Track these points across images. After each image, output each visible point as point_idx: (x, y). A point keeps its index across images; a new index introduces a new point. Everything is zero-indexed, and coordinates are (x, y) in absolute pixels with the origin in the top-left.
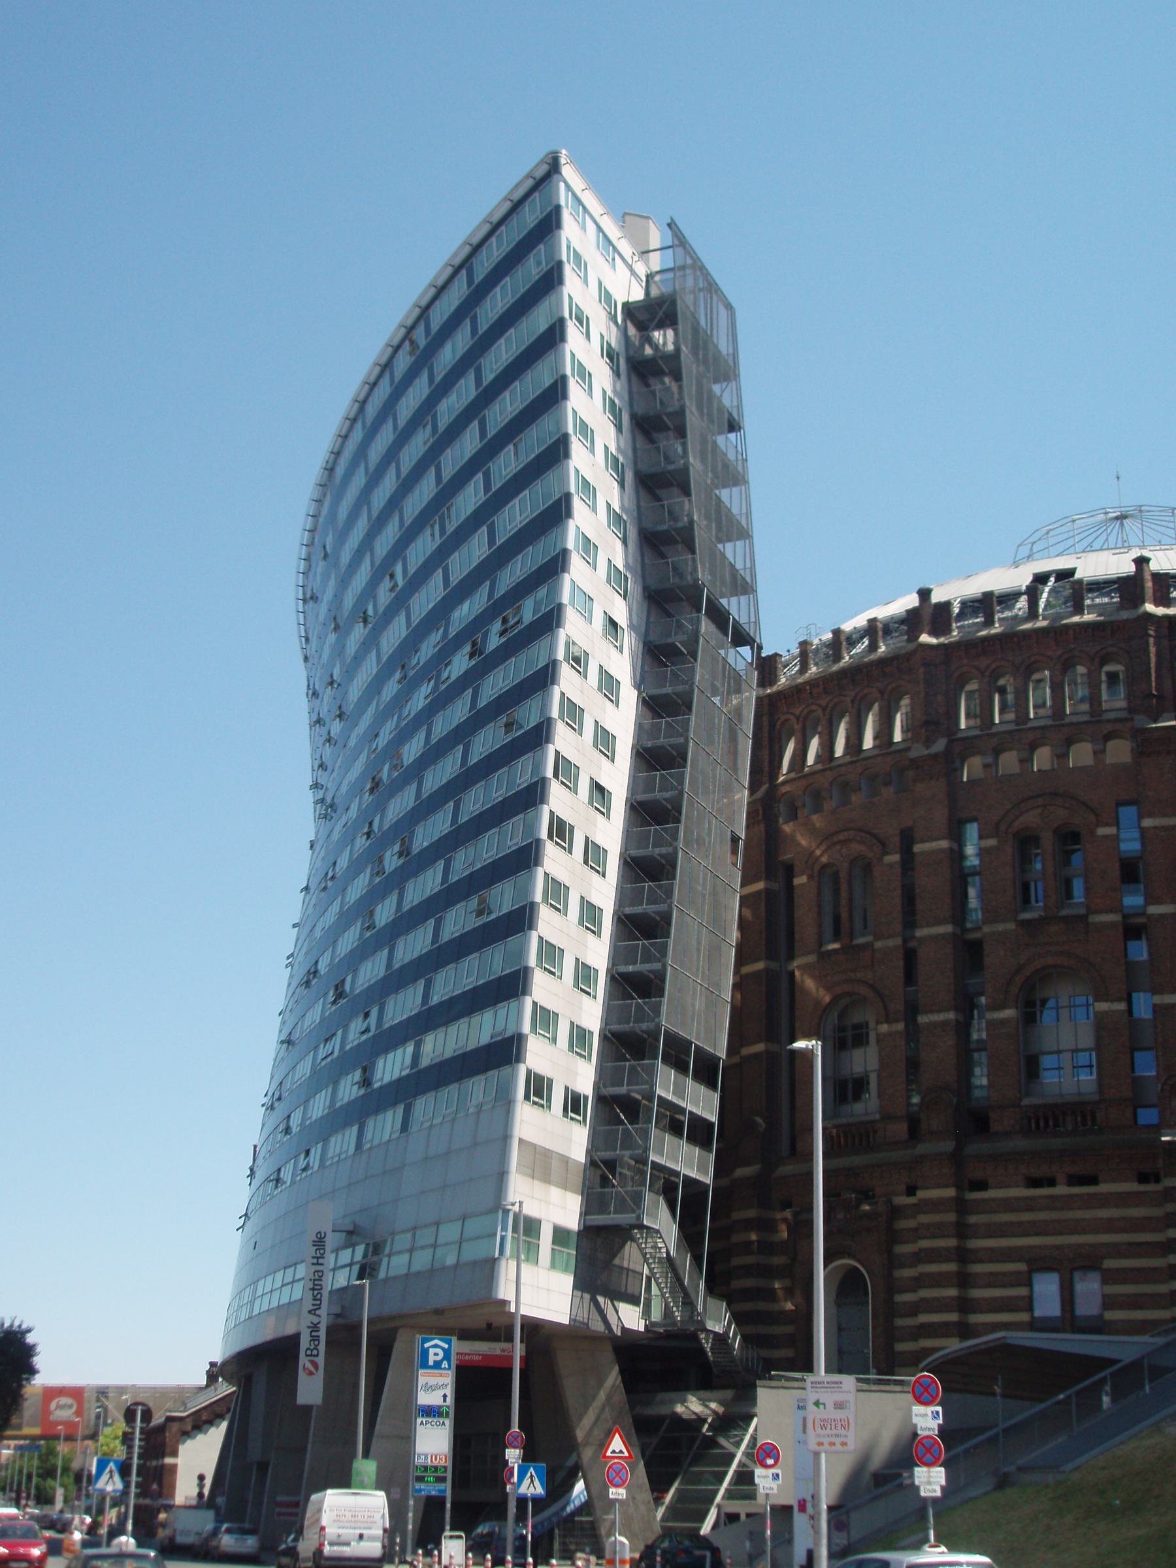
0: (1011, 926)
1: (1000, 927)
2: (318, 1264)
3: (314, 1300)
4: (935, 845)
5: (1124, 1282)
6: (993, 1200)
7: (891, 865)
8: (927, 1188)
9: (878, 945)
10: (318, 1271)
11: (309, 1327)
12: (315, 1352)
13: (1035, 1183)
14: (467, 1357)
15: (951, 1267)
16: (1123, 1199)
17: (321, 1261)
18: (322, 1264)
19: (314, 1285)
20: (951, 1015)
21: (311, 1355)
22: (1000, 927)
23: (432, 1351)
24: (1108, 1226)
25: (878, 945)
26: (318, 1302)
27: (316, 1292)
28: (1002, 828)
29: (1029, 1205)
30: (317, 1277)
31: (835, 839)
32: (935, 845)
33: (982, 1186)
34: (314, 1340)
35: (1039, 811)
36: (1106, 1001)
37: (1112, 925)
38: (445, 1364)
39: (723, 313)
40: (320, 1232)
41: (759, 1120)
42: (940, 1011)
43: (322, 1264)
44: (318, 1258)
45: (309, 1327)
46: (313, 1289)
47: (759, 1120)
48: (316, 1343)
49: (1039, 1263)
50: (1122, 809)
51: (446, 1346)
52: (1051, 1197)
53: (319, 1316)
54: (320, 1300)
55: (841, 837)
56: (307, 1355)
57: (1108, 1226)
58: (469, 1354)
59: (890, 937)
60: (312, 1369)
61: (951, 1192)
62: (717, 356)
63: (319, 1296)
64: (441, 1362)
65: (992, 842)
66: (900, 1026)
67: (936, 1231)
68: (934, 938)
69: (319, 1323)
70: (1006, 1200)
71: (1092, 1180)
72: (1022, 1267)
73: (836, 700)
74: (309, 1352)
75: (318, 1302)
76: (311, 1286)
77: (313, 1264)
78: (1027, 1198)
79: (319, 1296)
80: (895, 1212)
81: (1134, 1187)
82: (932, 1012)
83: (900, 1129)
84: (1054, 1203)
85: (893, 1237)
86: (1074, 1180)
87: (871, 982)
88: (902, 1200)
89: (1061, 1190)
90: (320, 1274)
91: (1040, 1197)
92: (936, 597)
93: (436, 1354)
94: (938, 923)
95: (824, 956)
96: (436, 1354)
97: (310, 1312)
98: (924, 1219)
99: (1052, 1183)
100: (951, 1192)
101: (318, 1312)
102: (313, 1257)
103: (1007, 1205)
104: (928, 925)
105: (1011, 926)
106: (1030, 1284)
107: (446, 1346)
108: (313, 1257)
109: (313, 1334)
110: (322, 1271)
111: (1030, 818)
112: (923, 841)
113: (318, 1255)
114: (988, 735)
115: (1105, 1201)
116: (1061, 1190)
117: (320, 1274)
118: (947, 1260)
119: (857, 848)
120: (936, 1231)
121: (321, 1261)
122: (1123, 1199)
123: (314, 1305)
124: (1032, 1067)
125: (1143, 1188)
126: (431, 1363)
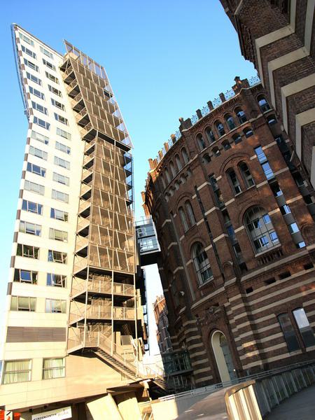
0: (233, 200)
15: (248, 323)
20: (223, 236)
25: (198, 224)
29: (268, 291)
33: (250, 290)
37: (265, 185)
50: (256, 150)
52: (276, 286)
61: (240, 296)
66: (211, 246)
67: (239, 311)
70: (260, 292)
71: (288, 275)
78: (266, 290)
80: (225, 309)
83: (221, 279)
84: (278, 288)
85: (228, 318)
86: (282, 277)
88: (226, 305)
89: (278, 282)
92: (184, 120)
95: (185, 234)
98: (233, 309)
99: (273, 281)
100: (240, 296)
111: (229, 165)
115: (295, 280)
116: (278, 282)
118: (246, 321)
119: (186, 198)
120: (239, 311)
124: (257, 245)
125: (308, 271)
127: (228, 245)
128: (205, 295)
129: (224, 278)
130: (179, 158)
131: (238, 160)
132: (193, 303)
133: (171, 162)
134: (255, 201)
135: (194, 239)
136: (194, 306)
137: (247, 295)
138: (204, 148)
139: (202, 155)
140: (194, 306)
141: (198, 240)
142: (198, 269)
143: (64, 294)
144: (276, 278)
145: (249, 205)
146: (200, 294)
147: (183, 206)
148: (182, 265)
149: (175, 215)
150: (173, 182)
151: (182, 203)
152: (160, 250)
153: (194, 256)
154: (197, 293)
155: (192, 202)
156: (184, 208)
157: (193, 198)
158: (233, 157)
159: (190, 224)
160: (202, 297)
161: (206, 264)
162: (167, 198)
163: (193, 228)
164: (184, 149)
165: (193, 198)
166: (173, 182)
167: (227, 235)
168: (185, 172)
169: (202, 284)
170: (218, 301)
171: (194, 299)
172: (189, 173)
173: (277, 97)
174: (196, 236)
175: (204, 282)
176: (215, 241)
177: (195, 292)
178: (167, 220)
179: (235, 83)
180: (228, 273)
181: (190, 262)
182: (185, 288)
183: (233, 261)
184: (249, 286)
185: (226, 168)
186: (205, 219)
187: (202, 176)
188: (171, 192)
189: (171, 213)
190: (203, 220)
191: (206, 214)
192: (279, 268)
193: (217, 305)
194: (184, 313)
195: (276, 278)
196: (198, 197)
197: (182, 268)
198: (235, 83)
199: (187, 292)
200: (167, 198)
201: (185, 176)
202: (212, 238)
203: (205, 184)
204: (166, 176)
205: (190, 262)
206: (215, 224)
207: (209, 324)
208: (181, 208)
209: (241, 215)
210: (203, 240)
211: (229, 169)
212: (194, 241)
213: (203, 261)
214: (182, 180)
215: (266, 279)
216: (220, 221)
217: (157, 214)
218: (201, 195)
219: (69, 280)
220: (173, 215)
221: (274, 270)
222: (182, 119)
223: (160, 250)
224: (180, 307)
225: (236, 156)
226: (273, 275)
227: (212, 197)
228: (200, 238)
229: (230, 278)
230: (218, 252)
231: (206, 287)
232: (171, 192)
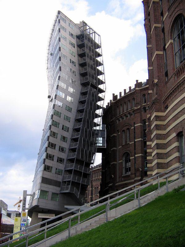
20: (141, 155)
25: (130, 143)
39: (97, 35)
41: (113, 176)
47: (113, 176)
62: (95, 44)
66: (134, 157)
83: (134, 175)
92: (139, 82)
95: (122, 146)
119: (128, 127)
127: (142, 160)
128: (124, 181)
129: (135, 176)
130: (130, 102)
132: (117, 183)
133: (125, 102)
136: (117, 184)
138: (145, 103)
139: (142, 107)
140: (117, 184)
141: (128, 151)
142: (124, 166)
143: (62, 167)
146: (122, 179)
147: (125, 130)
148: (116, 162)
149: (119, 133)
151: (125, 128)
152: (106, 147)
153: (124, 159)
154: (120, 178)
156: (125, 132)
157: (132, 128)
159: (126, 142)
160: (122, 181)
161: (129, 165)
162: (117, 121)
163: (127, 144)
164: (134, 99)
165: (132, 128)
167: (143, 155)
168: (131, 112)
169: (124, 175)
171: (118, 181)
172: (133, 114)
173: (180, 103)
174: (128, 149)
175: (125, 173)
176: (136, 156)
177: (119, 178)
178: (115, 135)
180: (138, 174)
181: (120, 161)
182: (115, 174)
183: (142, 169)
186: (135, 142)
188: (121, 119)
189: (118, 130)
190: (133, 142)
191: (136, 140)
194: (111, 187)
196: (134, 129)
197: (116, 163)
199: (115, 176)
200: (117, 121)
201: (131, 115)
202: (135, 154)
203: (140, 124)
204: (120, 109)
205: (120, 161)
206: (139, 148)
208: (124, 131)
210: (131, 153)
213: (128, 162)
214: (129, 115)
216: (141, 146)
217: (109, 127)
218: (136, 129)
219: (65, 161)
220: (118, 133)
223: (106, 147)
224: (109, 183)
227: (141, 133)
229: (138, 177)
230: (136, 162)
231: (124, 177)
232: (121, 119)
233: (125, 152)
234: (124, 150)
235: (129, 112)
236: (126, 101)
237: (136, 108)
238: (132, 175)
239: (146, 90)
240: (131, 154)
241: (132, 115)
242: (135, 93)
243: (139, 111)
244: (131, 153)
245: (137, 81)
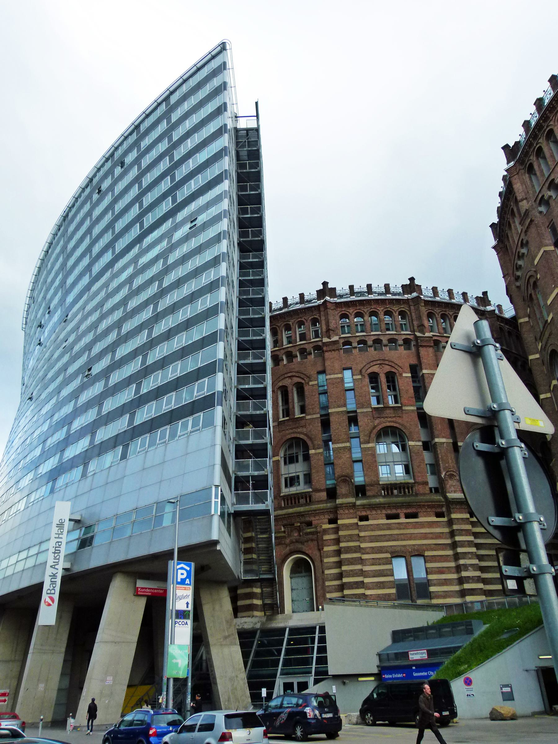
1: (365, 410)
2: (58, 538)
3: (54, 559)
4: (336, 376)
5: (435, 561)
6: (371, 525)
7: (313, 385)
8: (343, 519)
9: (308, 417)
10: (58, 542)
11: (50, 576)
12: (53, 591)
13: (389, 517)
14: (156, 591)
16: (431, 524)
17: (60, 536)
18: (62, 538)
19: (56, 550)
21: (50, 593)
22: (365, 410)
23: (180, 571)
24: (425, 536)
25: (308, 417)
26: (57, 561)
27: (56, 555)
28: (364, 371)
29: (389, 527)
30: (57, 546)
31: (286, 376)
32: (336, 376)
34: (53, 584)
35: (378, 366)
36: (413, 441)
38: (187, 581)
40: (61, 519)
42: (342, 442)
43: (62, 538)
44: (59, 534)
45: (50, 576)
46: (55, 553)
48: (54, 585)
49: (396, 554)
51: (188, 569)
53: (57, 569)
54: (59, 559)
55: (289, 375)
56: (47, 594)
57: (425, 536)
58: (157, 589)
59: (314, 414)
60: (51, 603)
63: (58, 557)
64: (185, 579)
65: (359, 377)
68: (338, 413)
69: (57, 573)
70: (378, 525)
71: (415, 516)
72: (389, 555)
73: (285, 323)
74: (49, 592)
75: (57, 561)
76: (54, 551)
77: (55, 538)
78: (387, 524)
79: (58, 557)
81: (435, 519)
82: (339, 443)
83: (324, 495)
84: (400, 526)
86: (407, 516)
87: (305, 433)
90: (60, 544)
91: (393, 523)
92: (330, 286)
93: (182, 574)
94: (339, 407)
96: (182, 574)
97: (51, 567)
99: (397, 517)
101: (56, 567)
102: (56, 534)
103: (379, 527)
104: (334, 408)
105: (370, 410)
106: (391, 563)
107: (188, 569)
108: (56, 534)
109: (52, 580)
110: (61, 542)
111: (375, 369)
112: (330, 374)
113: (60, 532)
114: (355, 336)
117: (60, 544)
121: (60, 536)
122: (431, 524)
123: (54, 562)
126: (179, 580)
131: (387, 369)
134: (399, 423)
135: (293, 433)
137: (361, 523)
139: (342, 341)
141: (302, 436)
144: (402, 515)
145: (388, 424)
150: (283, 351)
153: (282, 454)
155: (306, 388)
157: (311, 383)
158: (383, 362)
166: (283, 351)
168: (309, 348)
170: (312, 519)
179: (408, 282)
184: (364, 513)
185: (370, 371)
187: (337, 365)
191: (330, 411)
192: (408, 505)
193: (309, 524)
195: (402, 515)
198: (408, 282)
207: (292, 542)
209: (375, 431)
210: (311, 439)
211: (374, 373)
212: (293, 436)
215: (389, 512)
221: (402, 505)
222: (328, 283)
225: (387, 362)
226: (399, 511)
228: (306, 435)
229: (346, 496)
233: (289, 437)
234: (287, 432)
235: (302, 347)
236: (291, 323)
237: (325, 340)
238: (318, 494)
239: (349, 307)
240: (313, 443)
241: (310, 354)
242: (322, 309)
243: (334, 347)
244: (311, 439)
245: (325, 284)
